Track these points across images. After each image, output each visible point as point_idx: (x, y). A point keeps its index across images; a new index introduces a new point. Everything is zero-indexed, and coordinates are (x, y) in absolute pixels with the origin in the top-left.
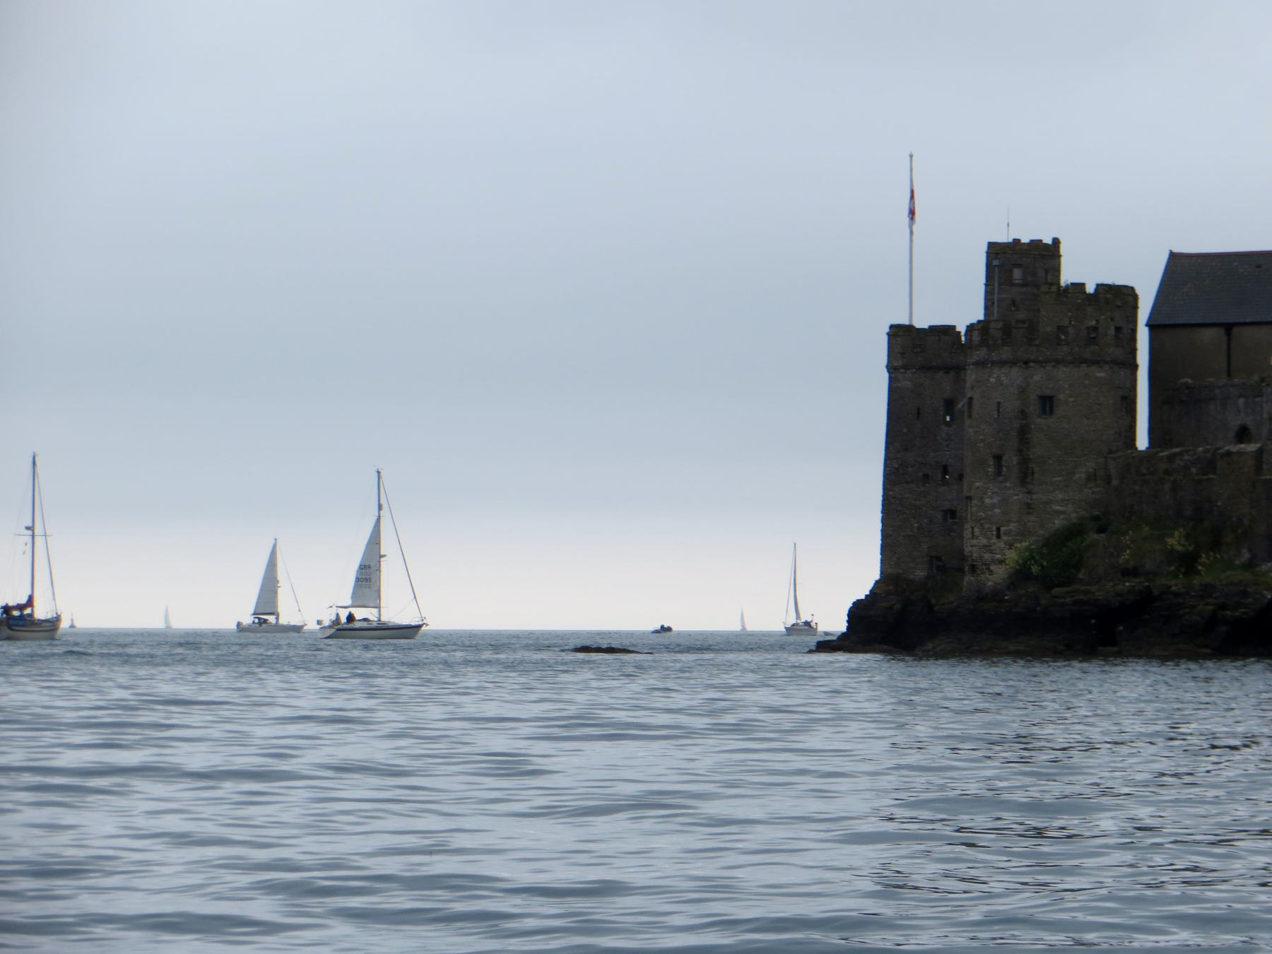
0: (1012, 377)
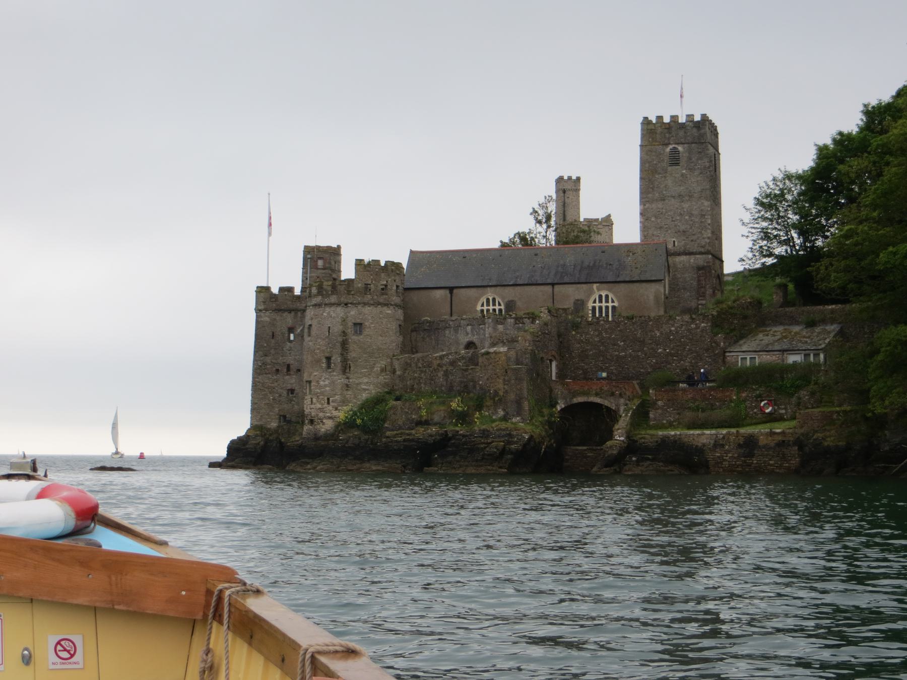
0: (340, 311)
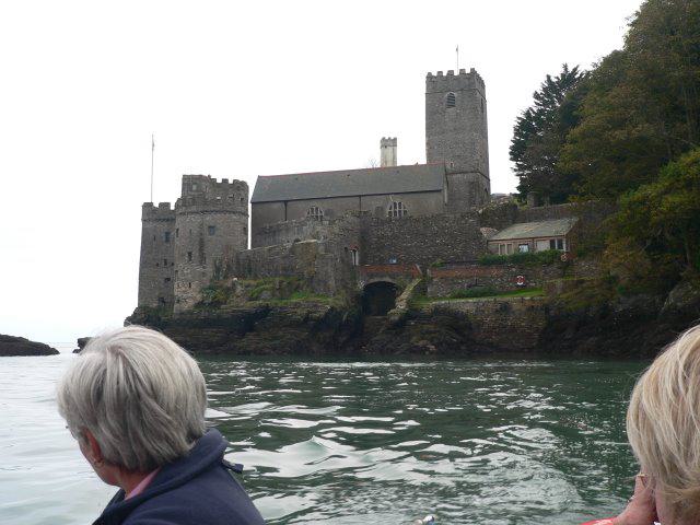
0: (197, 219)
